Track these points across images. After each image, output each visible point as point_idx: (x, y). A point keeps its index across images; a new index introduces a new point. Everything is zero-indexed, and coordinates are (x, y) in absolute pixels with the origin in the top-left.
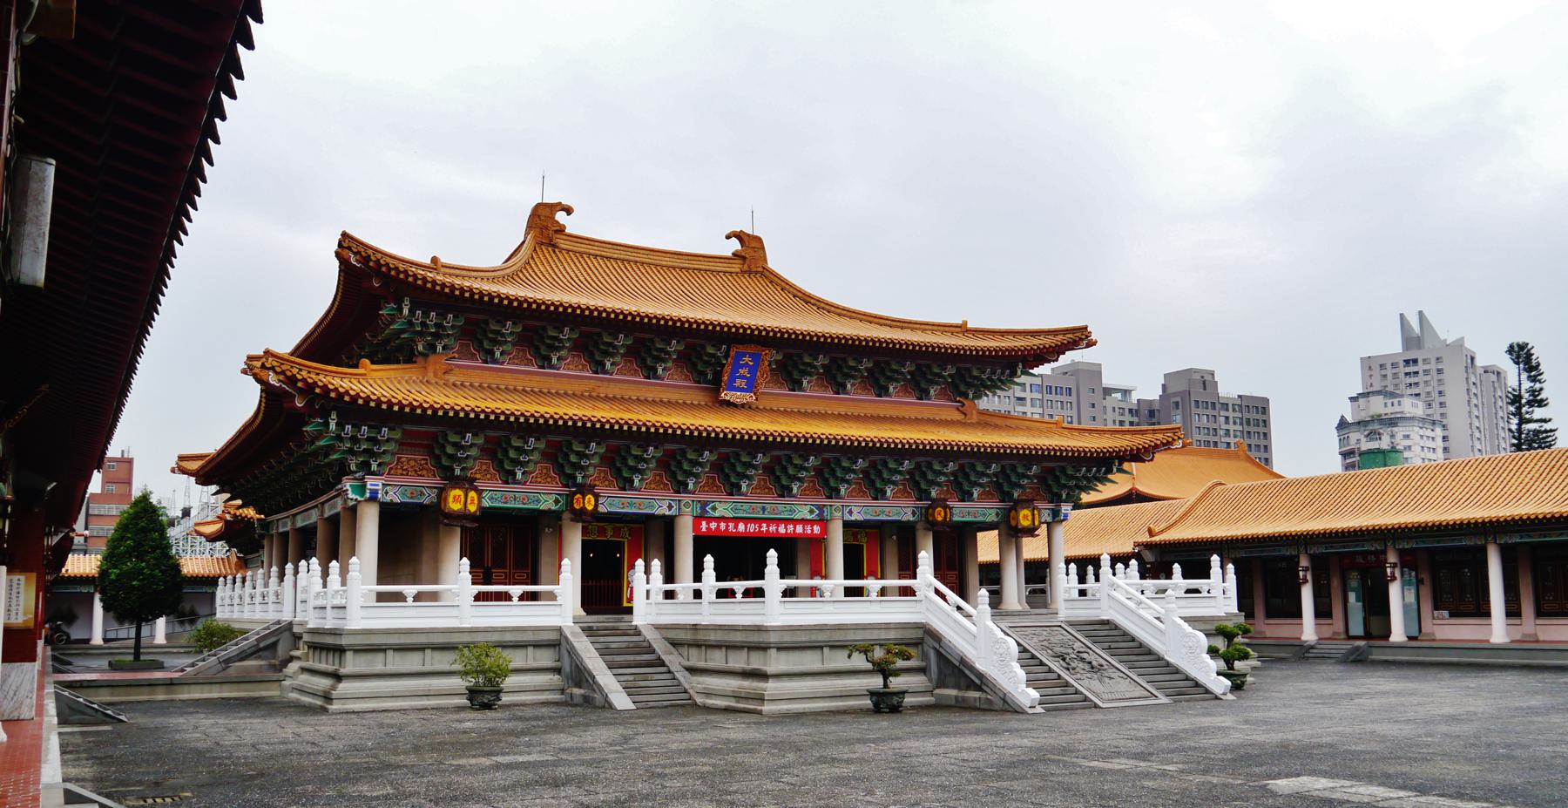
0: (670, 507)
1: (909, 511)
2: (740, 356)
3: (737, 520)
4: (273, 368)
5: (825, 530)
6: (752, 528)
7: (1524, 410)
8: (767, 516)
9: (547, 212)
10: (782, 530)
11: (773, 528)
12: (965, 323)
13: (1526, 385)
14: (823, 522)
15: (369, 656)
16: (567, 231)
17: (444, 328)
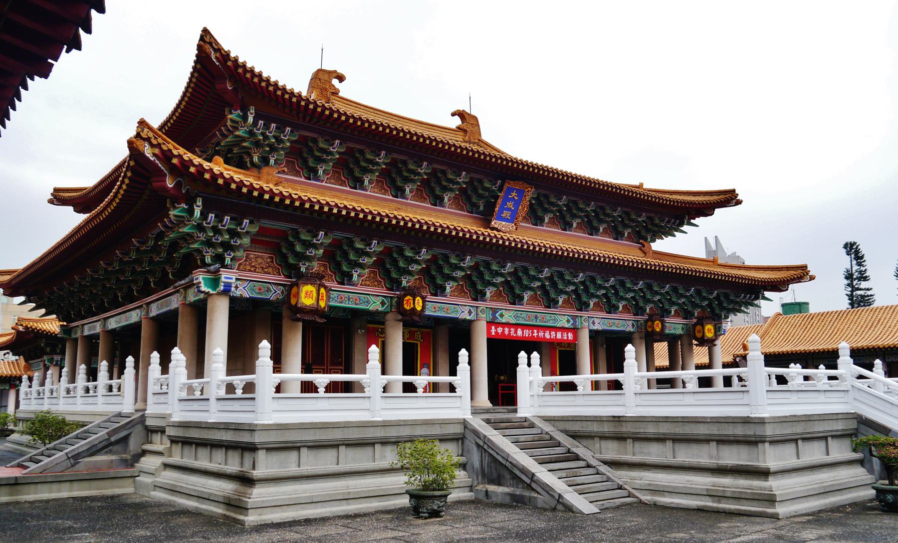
0: (470, 313)
1: (630, 323)
2: (511, 190)
3: (517, 326)
4: (148, 140)
5: (576, 337)
6: (527, 333)
7: (855, 283)
9: (326, 77)
11: (541, 334)
12: (642, 185)
13: (855, 268)
14: (575, 330)
15: (282, 455)
16: (340, 94)
17: (282, 141)
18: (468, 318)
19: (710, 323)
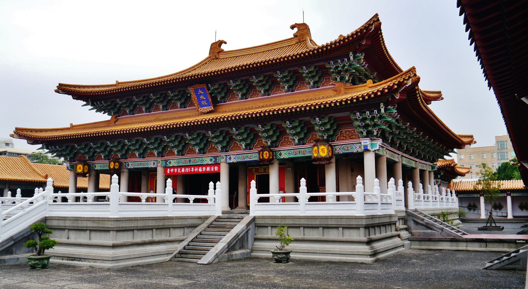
0: (154, 164)
6: (187, 170)
8: (191, 164)
10: (200, 170)
11: (196, 170)
14: (218, 165)
18: (153, 166)
19: (325, 145)
